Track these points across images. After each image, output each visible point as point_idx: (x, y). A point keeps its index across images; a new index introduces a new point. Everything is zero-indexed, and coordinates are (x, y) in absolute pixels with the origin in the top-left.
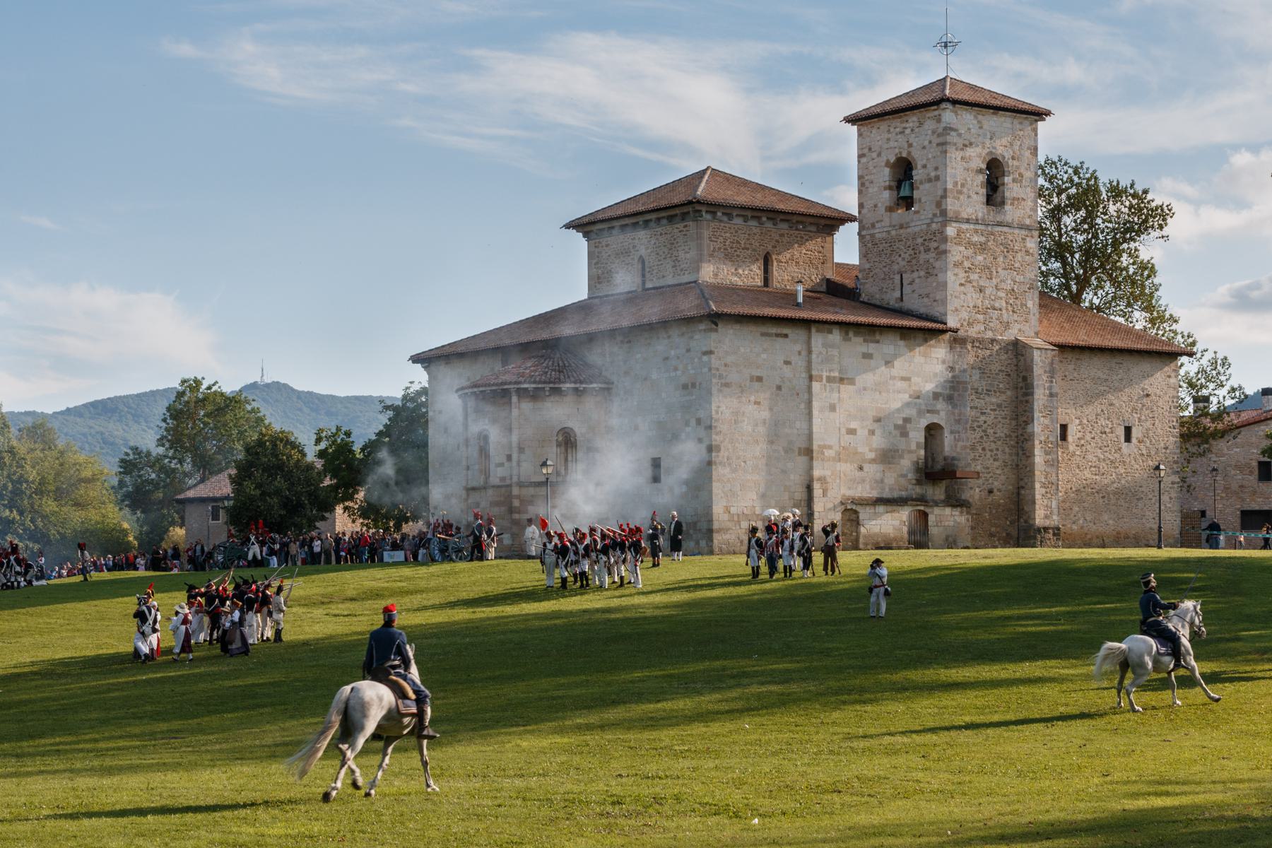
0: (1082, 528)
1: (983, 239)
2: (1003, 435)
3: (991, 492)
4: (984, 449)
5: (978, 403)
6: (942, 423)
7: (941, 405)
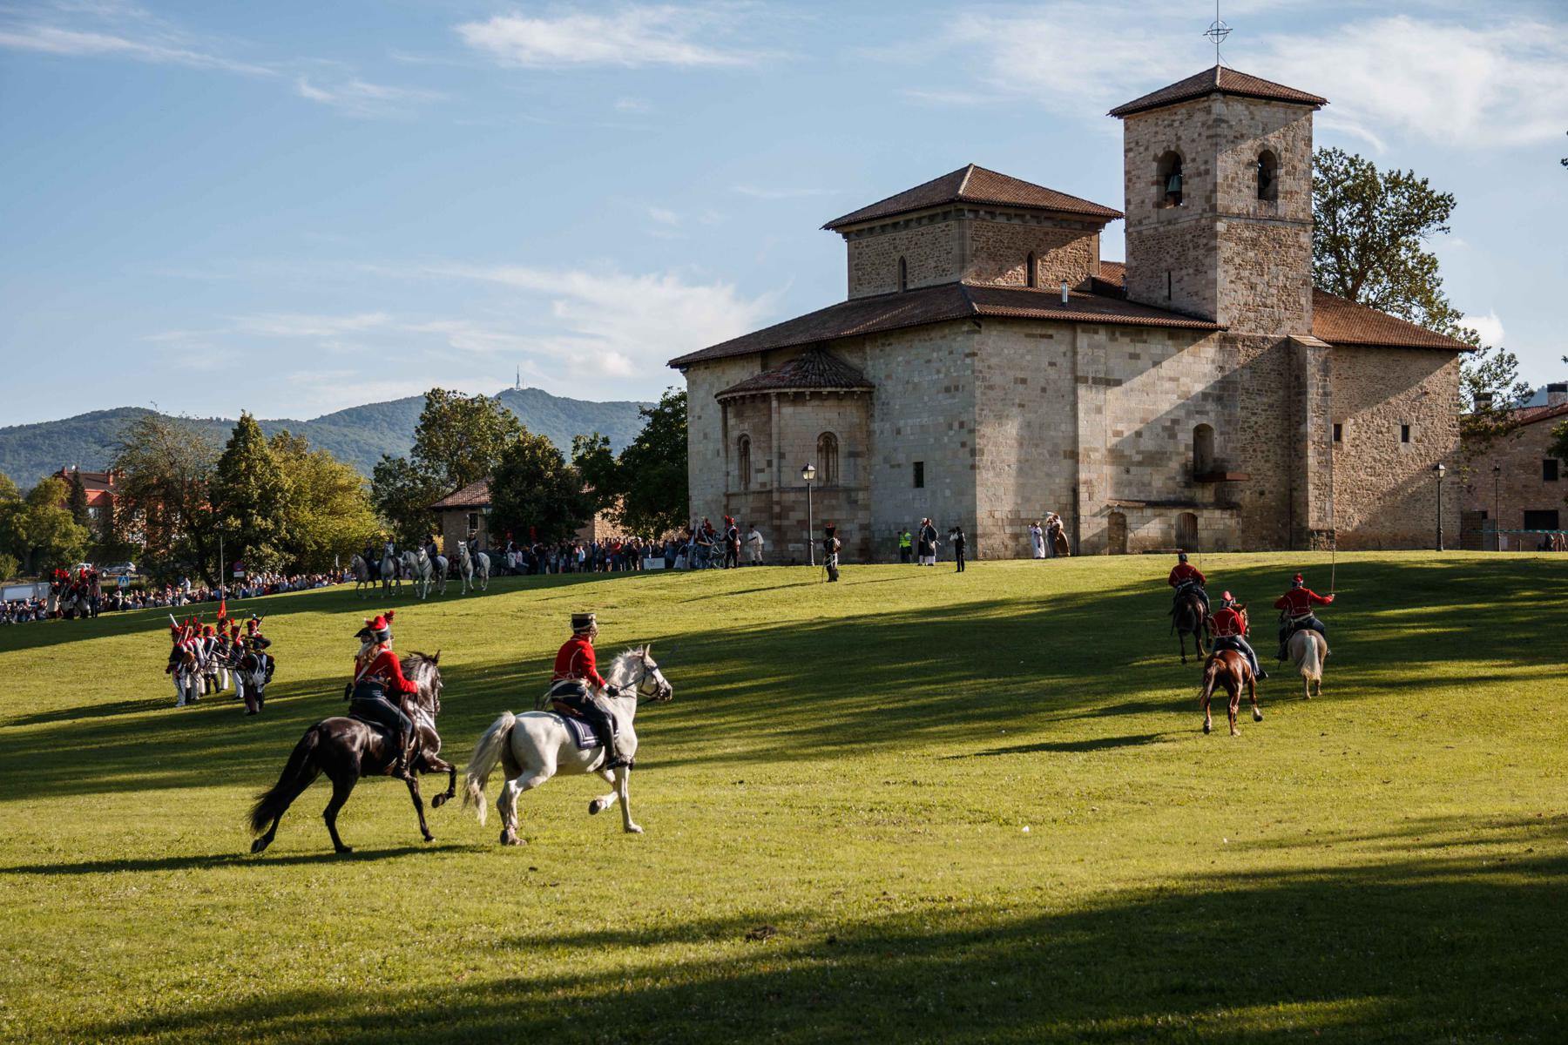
1: (1255, 234)
2: (1274, 436)
4: (1254, 450)
6: (1212, 425)
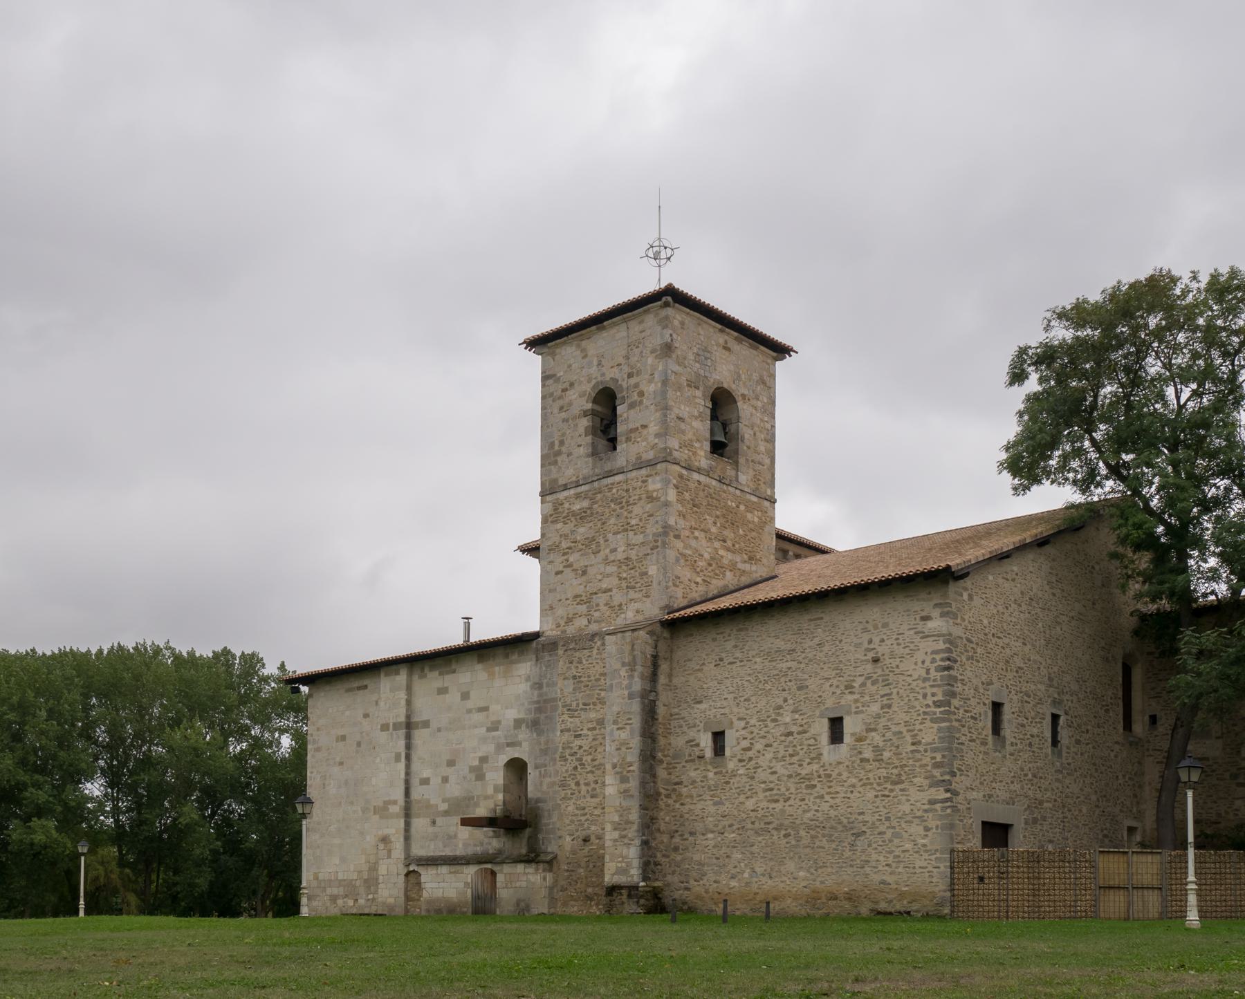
0: (747, 884)
1: (585, 504)
3: (586, 840)
4: (578, 784)
5: (570, 722)
7: (524, 735)
